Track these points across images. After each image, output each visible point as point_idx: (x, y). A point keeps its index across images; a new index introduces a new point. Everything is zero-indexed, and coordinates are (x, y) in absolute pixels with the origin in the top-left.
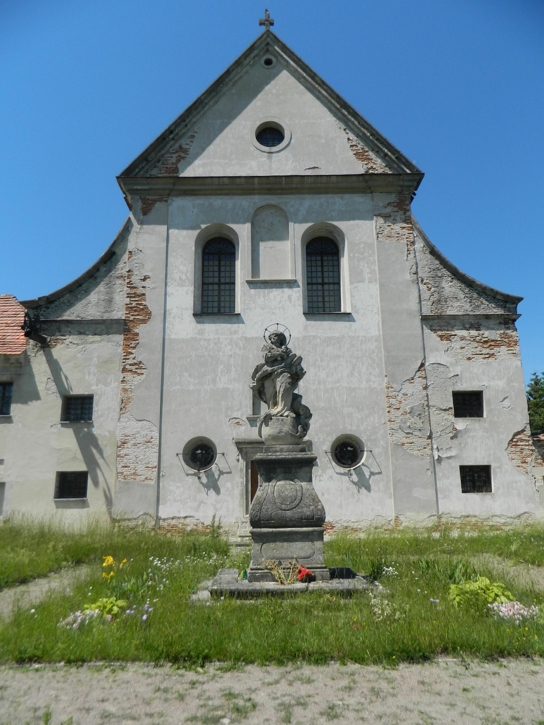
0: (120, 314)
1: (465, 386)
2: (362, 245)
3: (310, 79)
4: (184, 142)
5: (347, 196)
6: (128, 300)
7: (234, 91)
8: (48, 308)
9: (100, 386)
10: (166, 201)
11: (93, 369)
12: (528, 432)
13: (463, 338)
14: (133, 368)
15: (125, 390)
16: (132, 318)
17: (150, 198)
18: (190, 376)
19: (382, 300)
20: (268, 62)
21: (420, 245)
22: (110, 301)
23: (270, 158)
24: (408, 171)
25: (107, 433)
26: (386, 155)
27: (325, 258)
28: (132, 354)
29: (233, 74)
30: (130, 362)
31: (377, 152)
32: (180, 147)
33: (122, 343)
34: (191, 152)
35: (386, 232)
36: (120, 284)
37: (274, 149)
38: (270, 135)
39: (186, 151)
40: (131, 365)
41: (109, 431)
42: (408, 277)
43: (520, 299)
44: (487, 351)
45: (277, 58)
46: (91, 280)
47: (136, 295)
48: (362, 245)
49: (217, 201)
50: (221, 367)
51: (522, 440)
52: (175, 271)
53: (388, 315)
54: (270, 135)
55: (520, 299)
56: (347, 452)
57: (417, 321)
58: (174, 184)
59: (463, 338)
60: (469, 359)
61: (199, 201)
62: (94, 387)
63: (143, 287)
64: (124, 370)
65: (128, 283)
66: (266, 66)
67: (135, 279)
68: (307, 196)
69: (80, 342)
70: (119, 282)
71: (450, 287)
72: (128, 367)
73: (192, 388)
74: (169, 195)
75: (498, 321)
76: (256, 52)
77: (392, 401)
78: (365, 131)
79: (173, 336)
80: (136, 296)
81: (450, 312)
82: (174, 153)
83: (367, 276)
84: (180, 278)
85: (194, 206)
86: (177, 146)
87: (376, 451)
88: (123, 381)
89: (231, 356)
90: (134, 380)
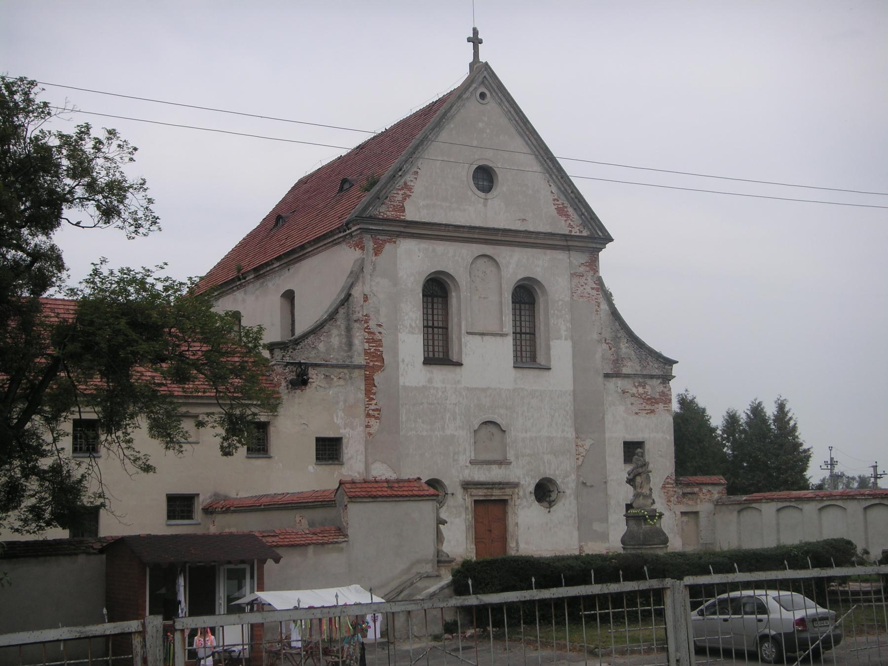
0: (360, 360)
1: (630, 438)
2: (560, 303)
3: (522, 124)
4: (408, 178)
5: (548, 251)
6: (366, 346)
7: (452, 126)
8: (294, 349)
9: (348, 430)
10: (395, 242)
11: (341, 414)
12: (674, 477)
13: (633, 395)
14: (376, 413)
15: (370, 434)
16: (371, 364)
17: (381, 238)
18: (423, 422)
19: (574, 356)
20: (483, 96)
21: (604, 306)
22: (350, 345)
23: (485, 205)
24: (600, 234)
25: (356, 474)
26: (583, 214)
27: (523, 306)
28: (373, 399)
29: (454, 108)
30: (373, 407)
31: (575, 209)
32: (405, 183)
33: (363, 387)
34: (415, 190)
35: (579, 292)
36: (358, 328)
37: (489, 195)
38: (485, 177)
39: (410, 189)
40: (373, 410)
41: (359, 473)
42: (595, 336)
43: (677, 362)
44: (648, 407)
45: (491, 94)
46: (331, 322)
47: (374, 341)
48: (560, 303)
49: (441, 247)
50: (448, 415)
51: (668, 483)
52: (406, 318)
53: (579, 370)
54: (485, 177)
55: (677, 362)
56: (545, 492)
57: (601, 379)
58: (405, 227)
59: (633, 395)
60: (637, 413)
61: (424, 245)
62: (342, 431)
63: (380, 333)
64: (368, 415)
65: (366, 328)
66: (481, 101)
67: (372, 324)
68: (516, 249)
69: (327, 386)
70: (356, 325)
71: (625, 348)
72: (371, 412)
73: (425, 434)
74: (398, 236)
75: (659, 381)
76: (474, 85)
77: (581, 450)
78: (568, 188)
79: (407, 384)
80: (374, 340)
81: (625, 371)
82: (400, 190)
83: (563, 333)
84: (411, 326)
85: (419, 250)
86: (403, 181)
87: (568, 492)
88: (367, 426)
89: (456, 404)
90: (375, 425)
